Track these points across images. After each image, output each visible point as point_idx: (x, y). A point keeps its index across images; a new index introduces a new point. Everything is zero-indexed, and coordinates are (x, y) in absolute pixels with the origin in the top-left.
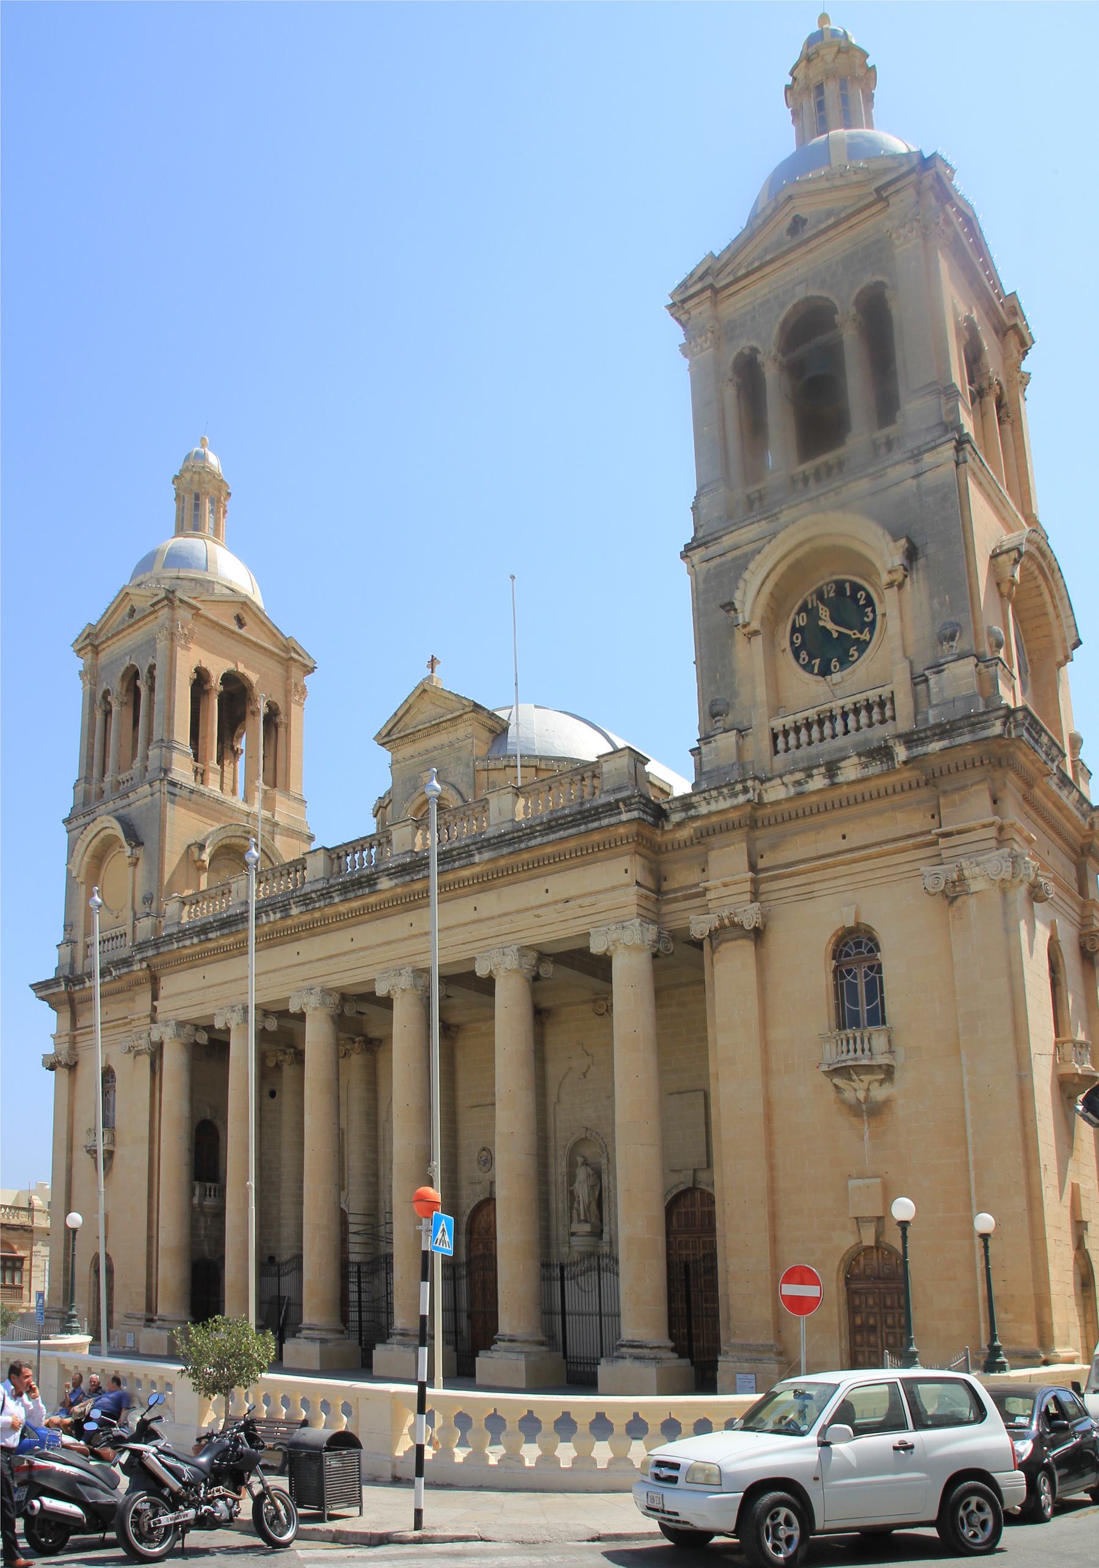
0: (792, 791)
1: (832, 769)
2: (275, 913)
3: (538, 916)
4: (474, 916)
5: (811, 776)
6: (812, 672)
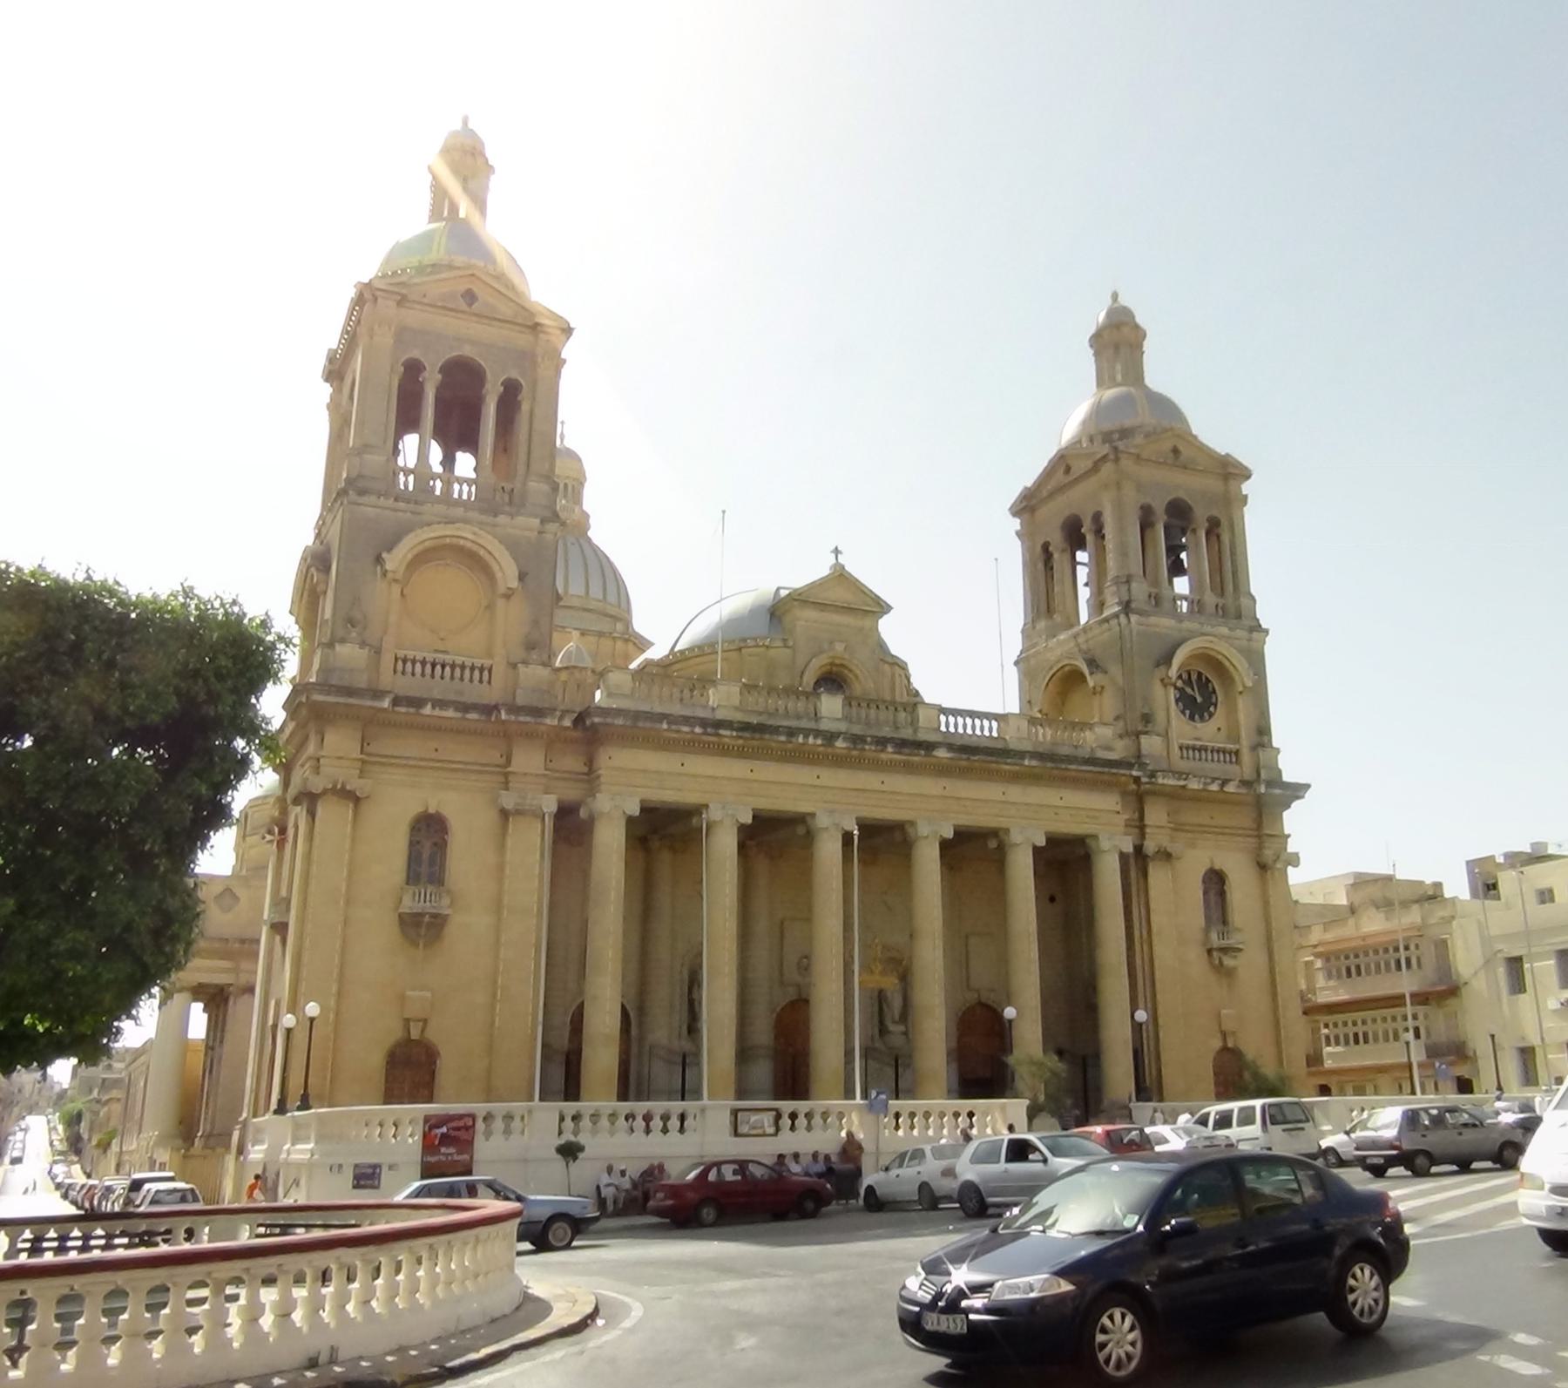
0: (1201, 786)
1: (1225, 782)
2: (815, 738)
3: (1056, 814)
4: (1003, 798)
5: (1213, 782)
6: (1185, 715)
